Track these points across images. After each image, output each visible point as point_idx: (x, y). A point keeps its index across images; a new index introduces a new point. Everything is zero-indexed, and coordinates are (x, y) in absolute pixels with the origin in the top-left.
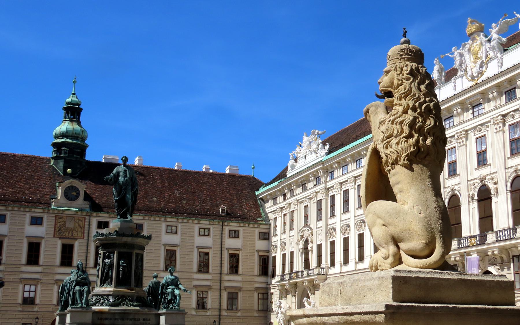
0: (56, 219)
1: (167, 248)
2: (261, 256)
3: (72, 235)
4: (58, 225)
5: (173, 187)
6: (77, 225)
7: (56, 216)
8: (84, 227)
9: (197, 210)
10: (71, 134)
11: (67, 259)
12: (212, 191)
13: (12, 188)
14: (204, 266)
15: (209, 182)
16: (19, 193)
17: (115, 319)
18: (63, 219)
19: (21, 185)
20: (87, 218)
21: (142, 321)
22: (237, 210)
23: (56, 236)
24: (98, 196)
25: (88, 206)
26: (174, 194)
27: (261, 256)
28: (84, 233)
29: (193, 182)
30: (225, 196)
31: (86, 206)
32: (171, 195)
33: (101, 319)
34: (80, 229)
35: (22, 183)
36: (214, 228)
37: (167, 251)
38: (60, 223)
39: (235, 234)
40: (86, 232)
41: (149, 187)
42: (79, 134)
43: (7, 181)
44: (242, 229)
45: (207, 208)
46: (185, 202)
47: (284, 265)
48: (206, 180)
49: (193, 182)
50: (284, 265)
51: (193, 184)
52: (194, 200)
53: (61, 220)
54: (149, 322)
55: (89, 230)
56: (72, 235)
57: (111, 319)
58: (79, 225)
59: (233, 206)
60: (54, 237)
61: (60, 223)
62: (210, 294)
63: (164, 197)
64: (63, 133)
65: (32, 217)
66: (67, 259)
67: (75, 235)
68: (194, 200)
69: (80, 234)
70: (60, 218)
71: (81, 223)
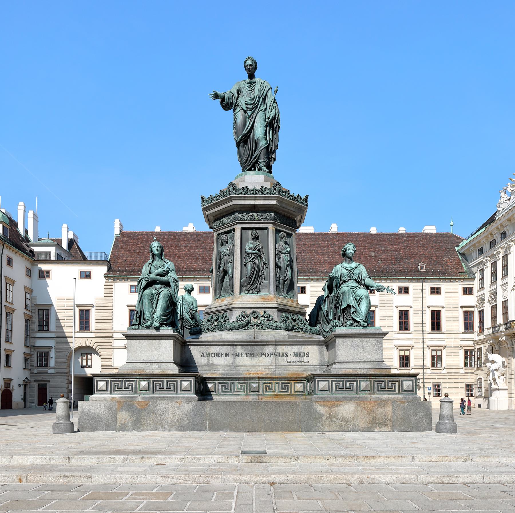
2: (465, 312)
9: (395, 269)
17: (237, 355)
21: (291, 358)
22: (437, 267)
27: (465, 312)
32: (366, 257)
33: (208, 355)
36: (414, 286)
39: (435, 291)
44: (444, 286)
45: (405, 266)
47: (494, 317)
50: (494, 317)
52: (391, 260)
54: (306, 359)
57: (228, 355)
59: (432, 263)
68: (391, 260)
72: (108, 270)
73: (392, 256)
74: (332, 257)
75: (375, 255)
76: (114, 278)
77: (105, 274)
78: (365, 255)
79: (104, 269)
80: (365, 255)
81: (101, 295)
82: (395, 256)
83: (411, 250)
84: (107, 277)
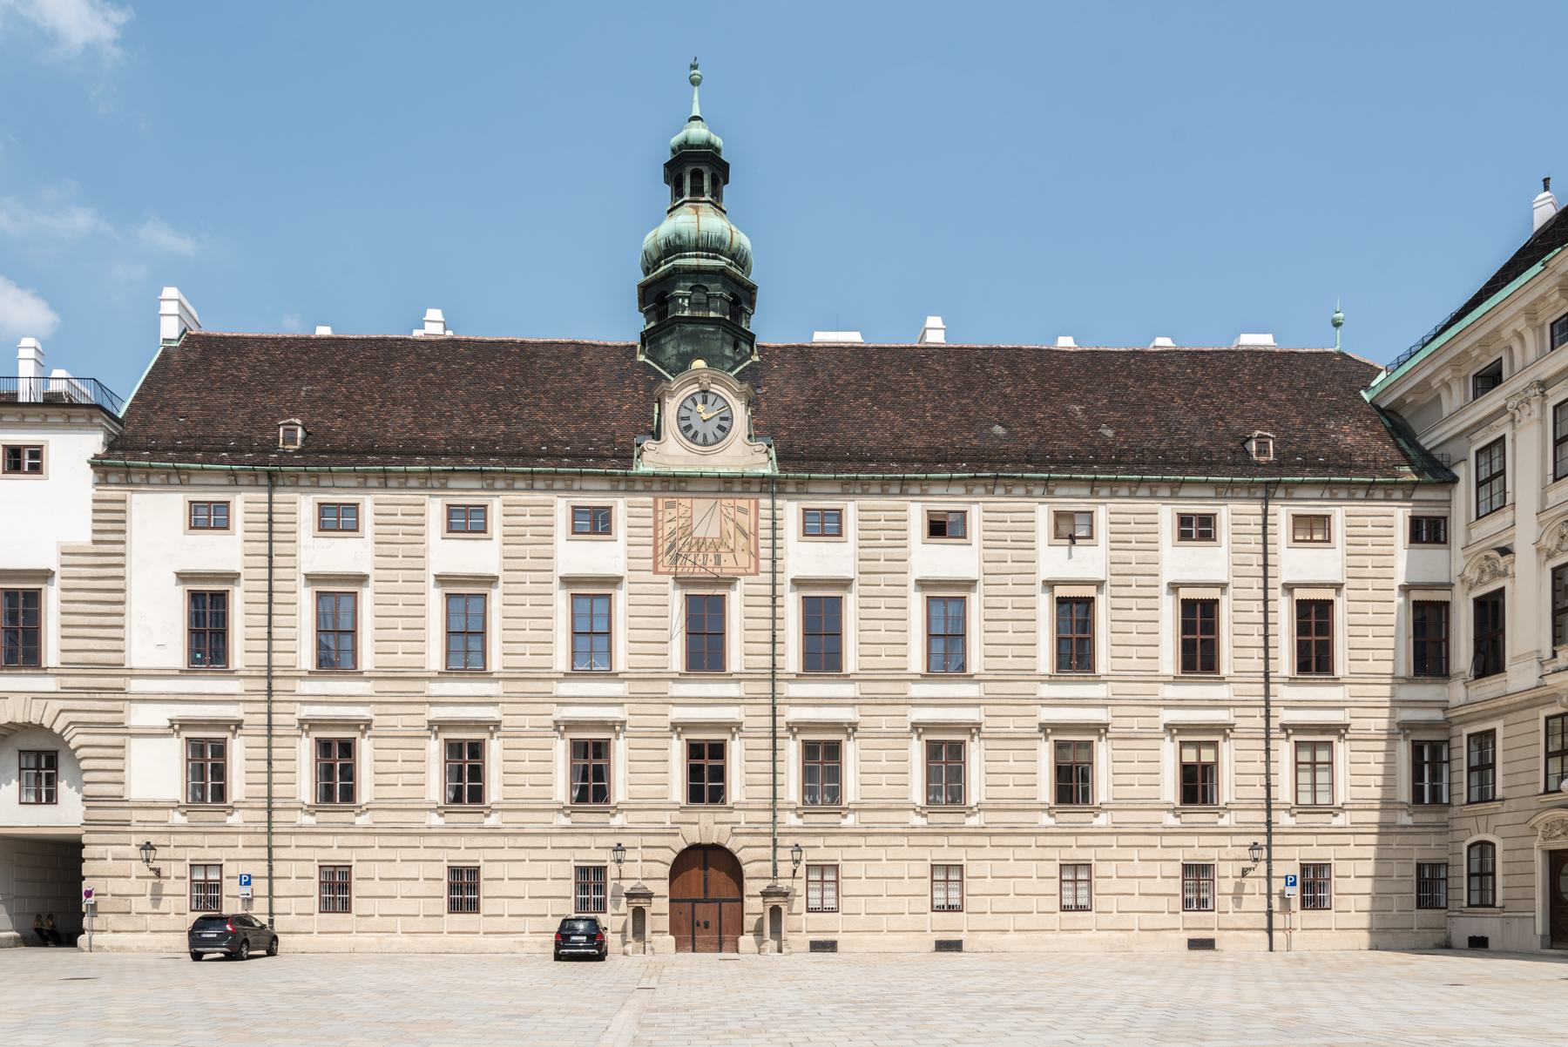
0: (656, 511)
1: (1061, 591)
3: (718, 563)
4: (667, 531)
5: (1058, 395)
6: (731, 526)
7: (656, 503)
8: (756, 534)
10: (693, 244)
11: (706, 648)
12: (1203, 396)
13: (508, 425)
14: (1199, 653)
15: (1184, 373)
16: (531, 434)
18: (682, 510)
19: (540, 416)
20: (765, 502)
23: (660, 568)
24: (797, 432)
25: (764, 458)
26: (1065, 413)
28: (756, 555)
29: (1126, 377)
30: (1254, 409)
31: (762, 463)
32: (1055, 416)
34: (742, 540)
35: (542, 409)
37: (1061, 601)
38: (673, 525)
40: (765, 553)
41: (975, 400)
42: (721, 240)
43: (495, 405)
46: (1109, 433)
48: (1172, 369)
49: (1128, 376)
51: (1130, 382)
53: (674, 512)
55: (774, 548)
56: (718, 563)
58: (737, 526)
60: (656, 572)
61: (673, 525)
62: (1227, 751)
63: (1034, 424)
64: (668, 243)
65: (574, 507)
66: (706, 648)
67: (727, 560)
69: (744, 560)
70: (669, 506)
71: (745, 521)
72: (112, 446)
73: (1146, 413)
74: (933, 417)
75: (1085, 412)
76: (127, 476)
77: (96, 457)
78: (1050, 409)
79: (93, 442)
80: (1050, 409)
81: (81, 533)
82: (1155, 414)
83: (1207, 396)
84: (101, 467)
